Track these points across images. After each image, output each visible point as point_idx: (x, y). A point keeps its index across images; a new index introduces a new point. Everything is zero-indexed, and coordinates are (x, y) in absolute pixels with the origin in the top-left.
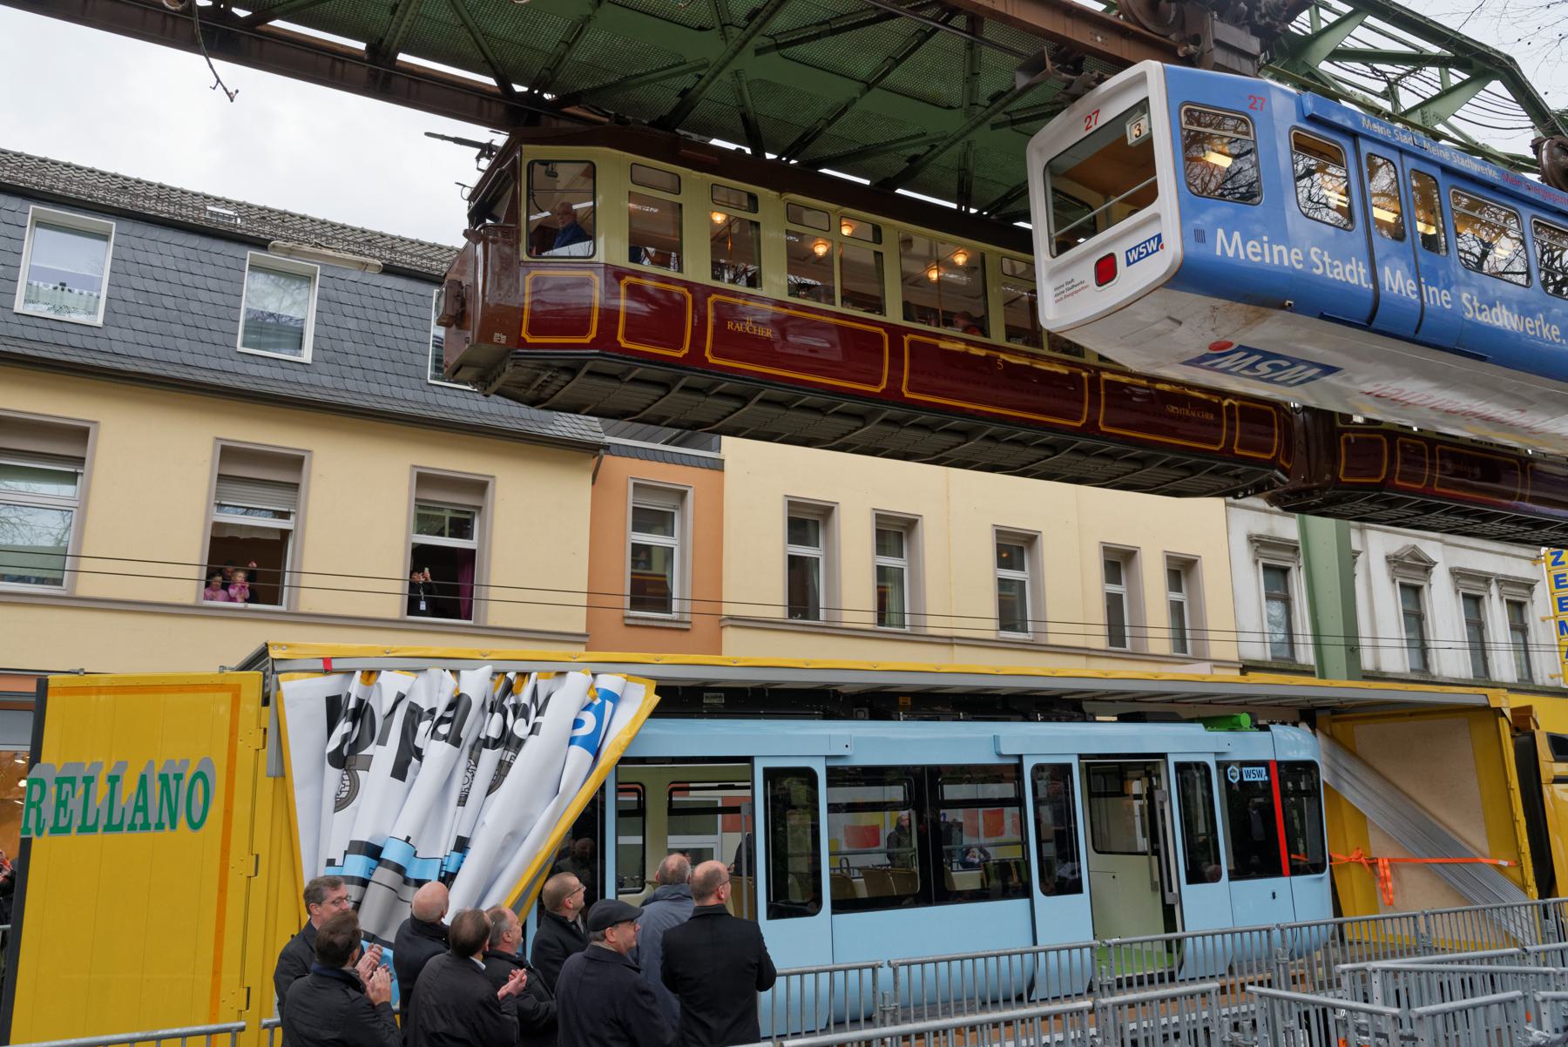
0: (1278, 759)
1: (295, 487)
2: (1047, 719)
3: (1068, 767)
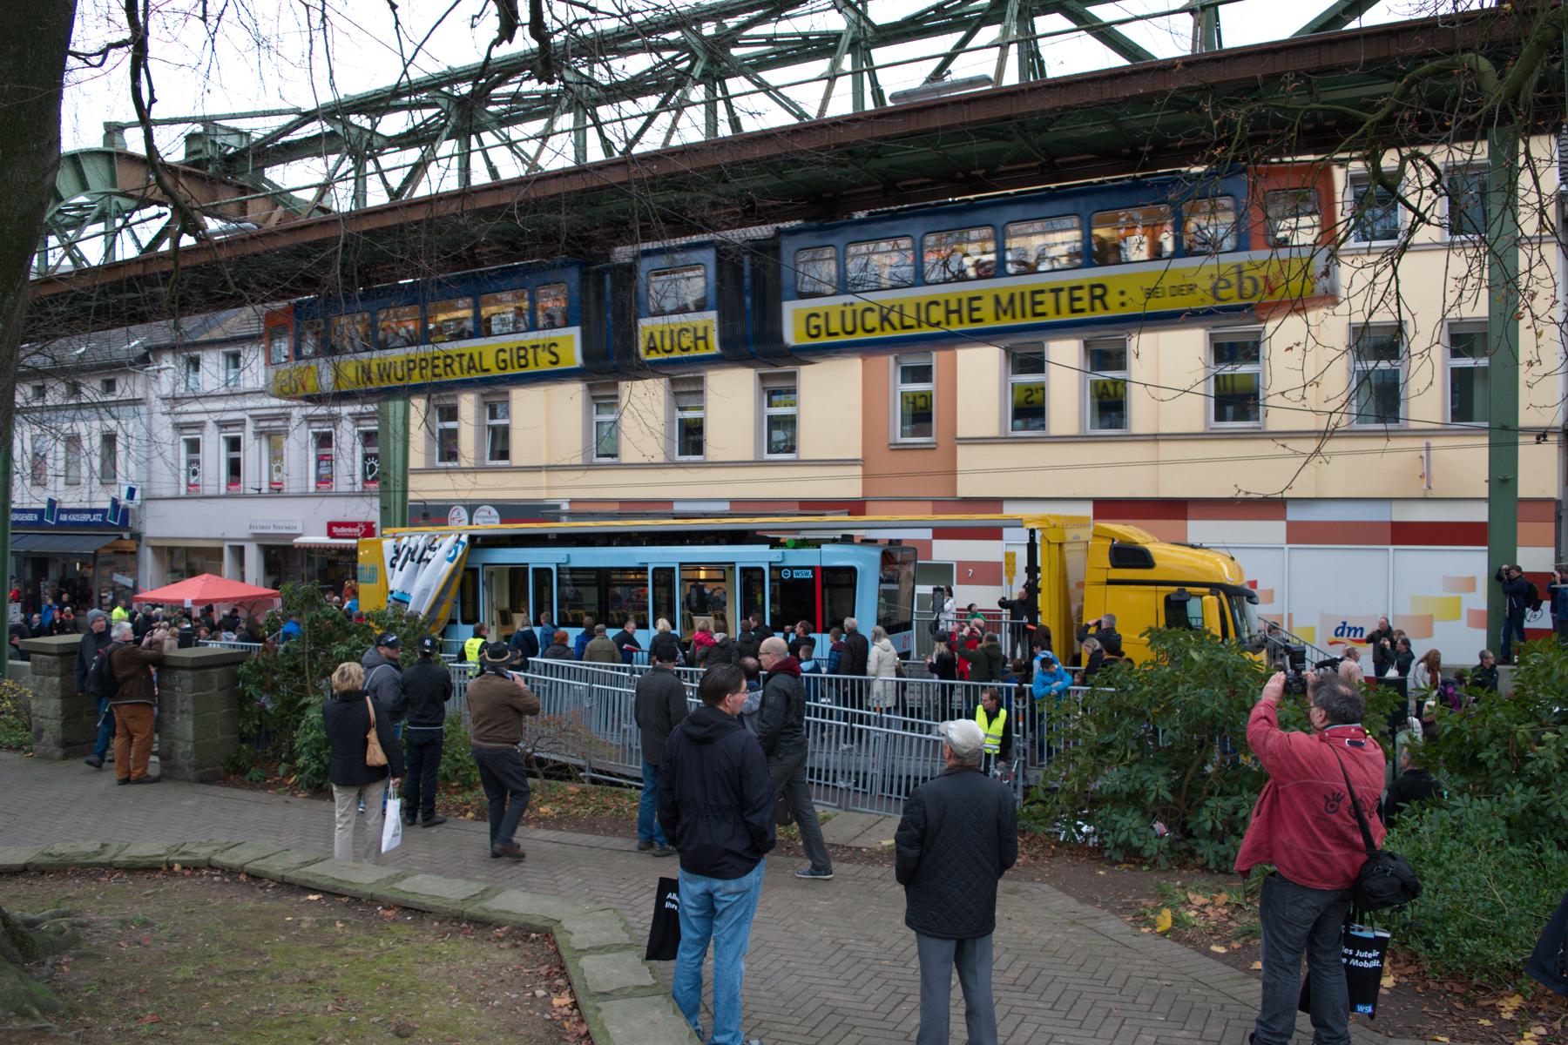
0: (824, 564)
1: (701, 392)
2: (691, 544)
3: (673, 569)
